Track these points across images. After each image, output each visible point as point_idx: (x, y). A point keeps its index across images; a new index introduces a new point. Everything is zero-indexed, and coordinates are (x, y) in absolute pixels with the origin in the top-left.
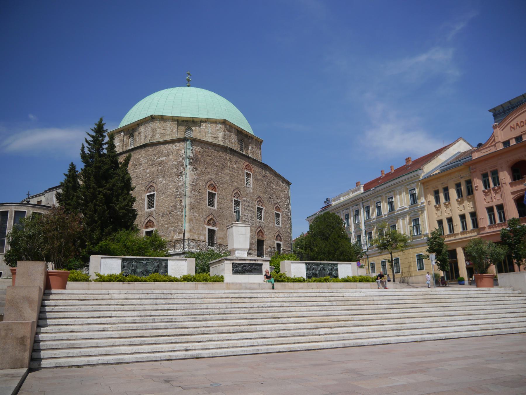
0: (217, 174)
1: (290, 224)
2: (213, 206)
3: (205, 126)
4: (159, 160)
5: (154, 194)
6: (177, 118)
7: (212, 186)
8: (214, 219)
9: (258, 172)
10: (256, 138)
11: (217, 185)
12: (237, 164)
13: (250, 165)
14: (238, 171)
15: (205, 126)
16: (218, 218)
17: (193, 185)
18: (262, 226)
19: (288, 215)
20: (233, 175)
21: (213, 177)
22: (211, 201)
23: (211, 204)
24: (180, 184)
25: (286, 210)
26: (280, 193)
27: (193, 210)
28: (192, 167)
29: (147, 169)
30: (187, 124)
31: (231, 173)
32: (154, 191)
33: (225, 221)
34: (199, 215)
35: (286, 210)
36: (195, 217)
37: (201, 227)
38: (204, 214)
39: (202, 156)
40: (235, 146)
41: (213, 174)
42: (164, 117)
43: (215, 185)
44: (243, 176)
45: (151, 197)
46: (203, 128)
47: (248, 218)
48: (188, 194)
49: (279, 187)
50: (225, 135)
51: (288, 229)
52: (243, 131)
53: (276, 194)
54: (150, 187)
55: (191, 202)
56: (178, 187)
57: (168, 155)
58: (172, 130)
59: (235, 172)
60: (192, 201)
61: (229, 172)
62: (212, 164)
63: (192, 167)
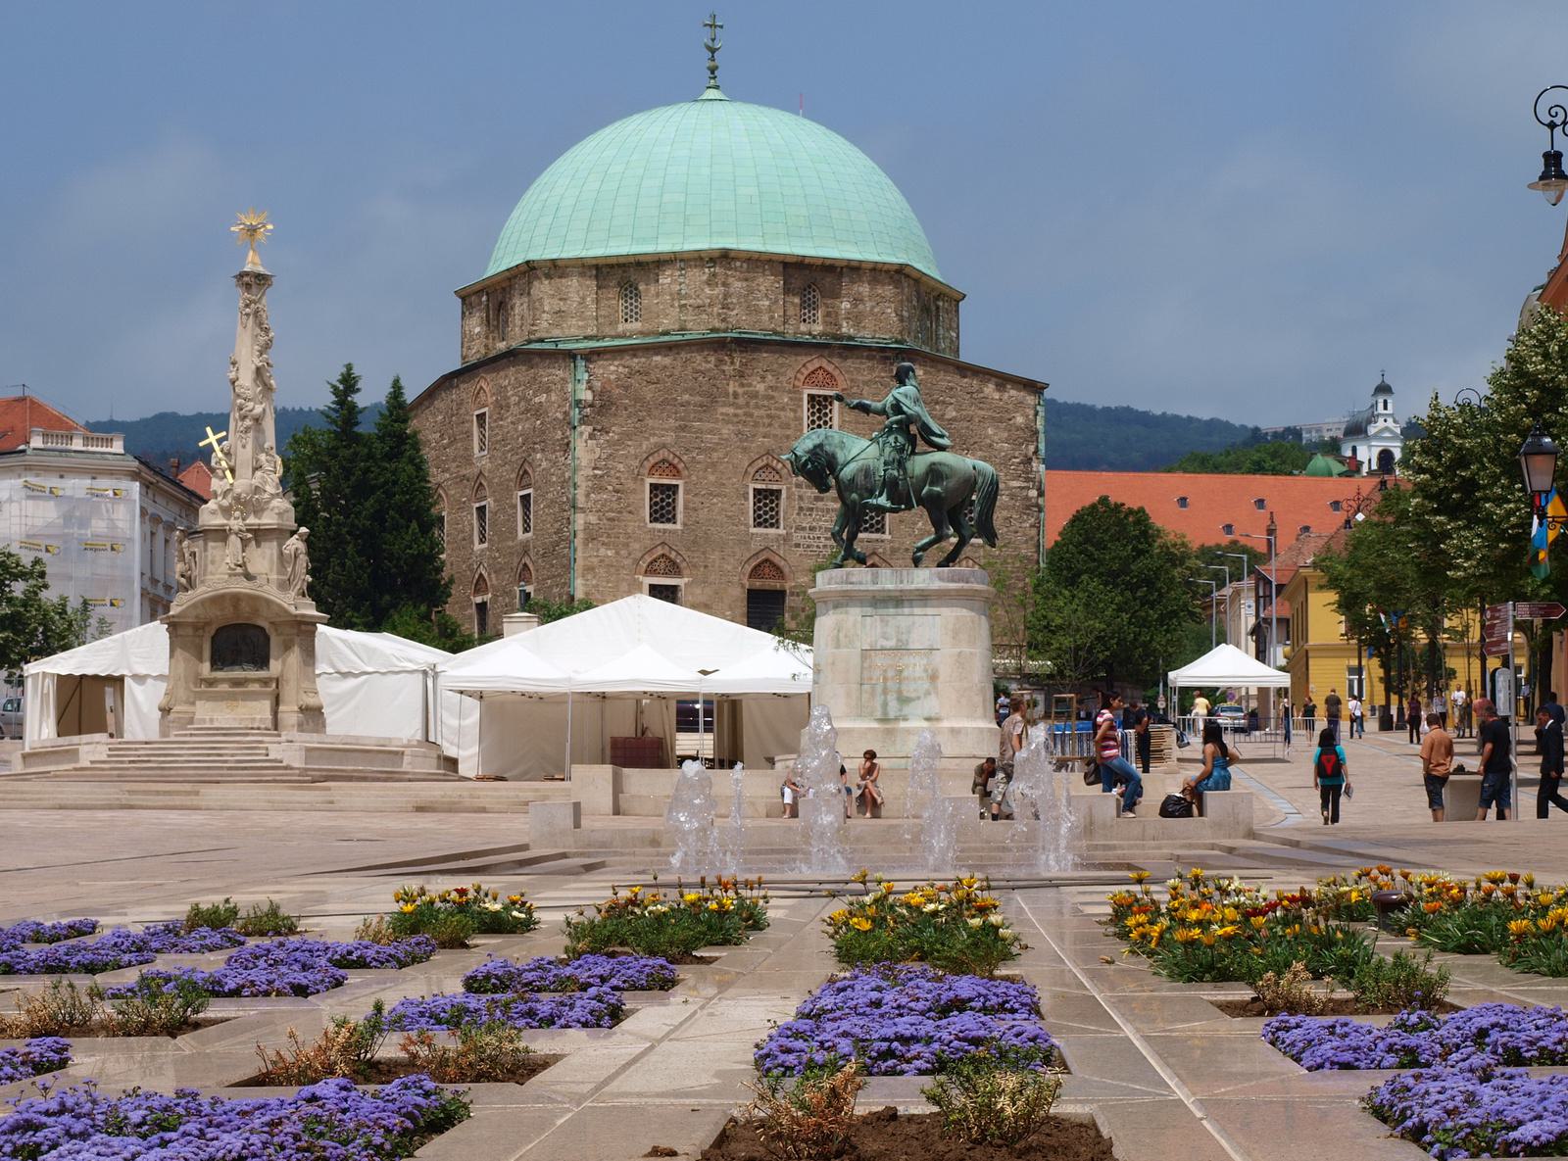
0: (683, 428)
1: (1032, 526)
2: (673, 520)
3: (671, 275)
4: (537, 400)
5: (529, 495)
6: (594, 262)
7: (667, 465)
8: (673, 555)
9: (865, 383)
10: (871, 266)
11: (685, 458)
12: (770, 377)
13: (830, 368)
14: (773, 397)
15: (671, 275)
16: (688, 550)
17: (595, 476)
18: (881, 550)
19: (1027, 498)
20: (751, 415)
21: (670, 438)
22: (662, 508)
23: (662, 516)
24: (567, 475)
25: (1015, 484)
26: (985, 429)
27: (595, 542)
28: (590, 429)
29: (519, 420)
30: (624, 272)
31: (739, 411)
32: (528, 486)
33: (715, 556)
34: (617, 553)
35: (1015, 484)
36: (601, 561)
37: (625, 584)
38: (637, 546)
39: (626, 388)
40: (772, 317)
41: (667, 430)
42: (559, 263)
43: (676, 461)
44: (795, 411)
45: (526, 499)
46: (665, 281)
47: (817, 533)
48: (581, 501)
49: (981, 409)
50: (726, 296)
51: (1025, 546)
52: (807, 261)
53: (961, 436)
54: (523, 478)
55: (587, 526)
56: (564, 483)
57: (548, 391)
58: (583, 298)
59: (757, 407)
60: (593, 519)
61: (731, 411)
62: (666, 402)
63: (590, 429)
